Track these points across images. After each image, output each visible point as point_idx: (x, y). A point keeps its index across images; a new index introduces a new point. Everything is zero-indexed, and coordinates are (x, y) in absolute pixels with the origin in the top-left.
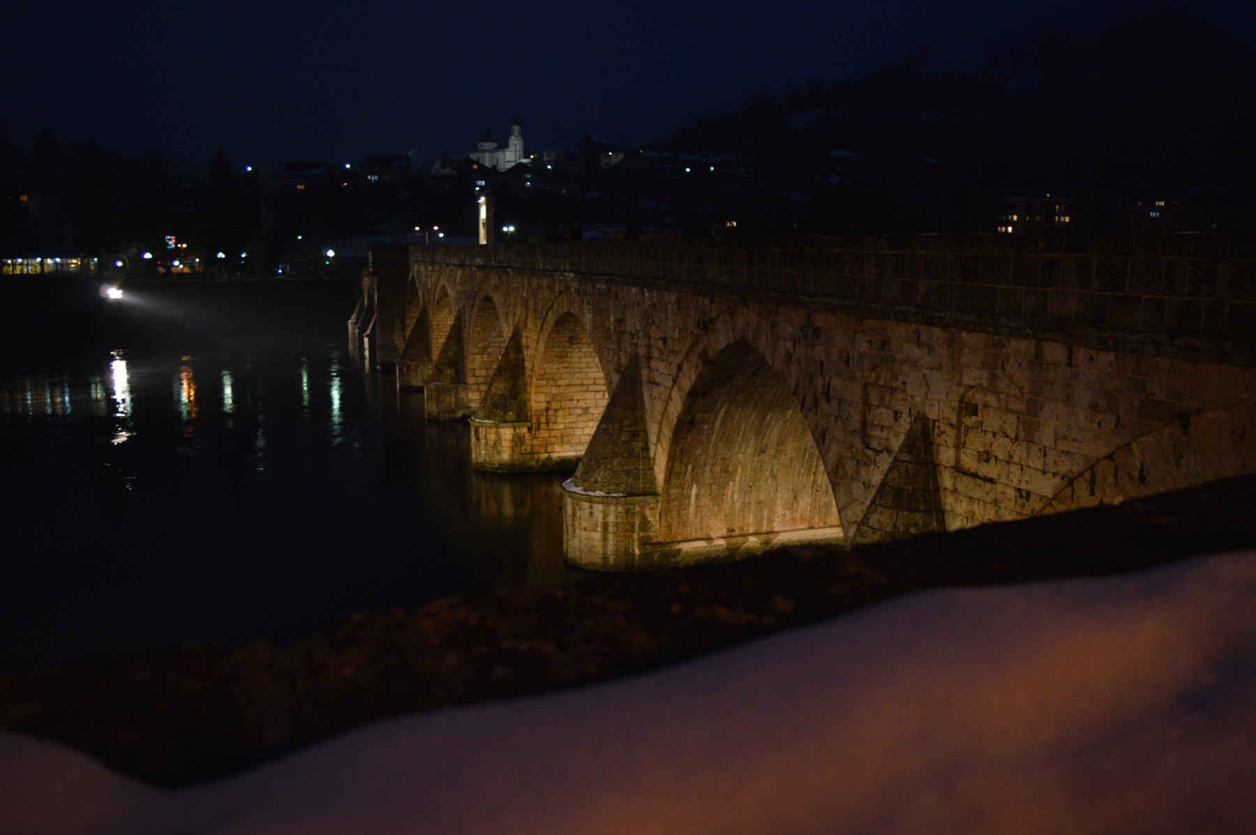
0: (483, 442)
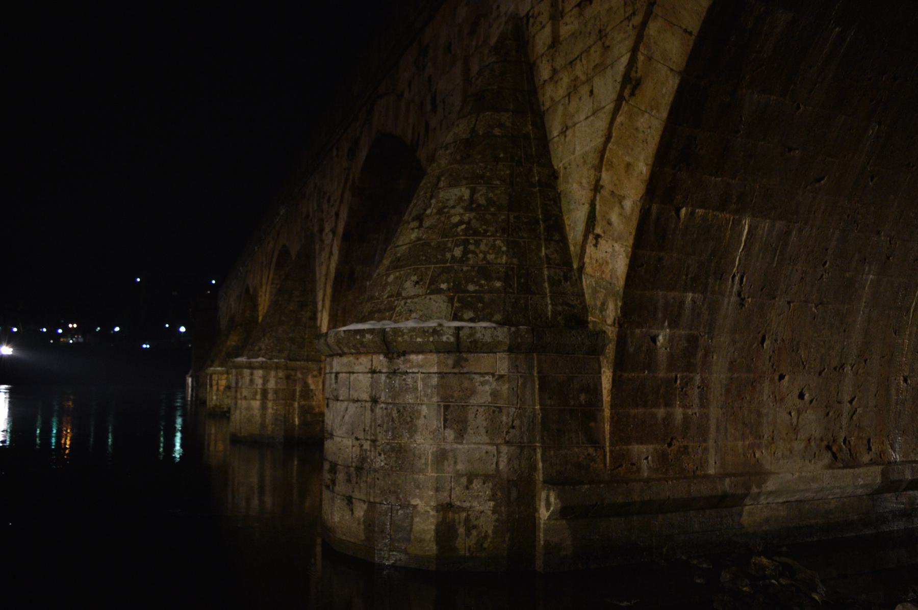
0: (215, 388)
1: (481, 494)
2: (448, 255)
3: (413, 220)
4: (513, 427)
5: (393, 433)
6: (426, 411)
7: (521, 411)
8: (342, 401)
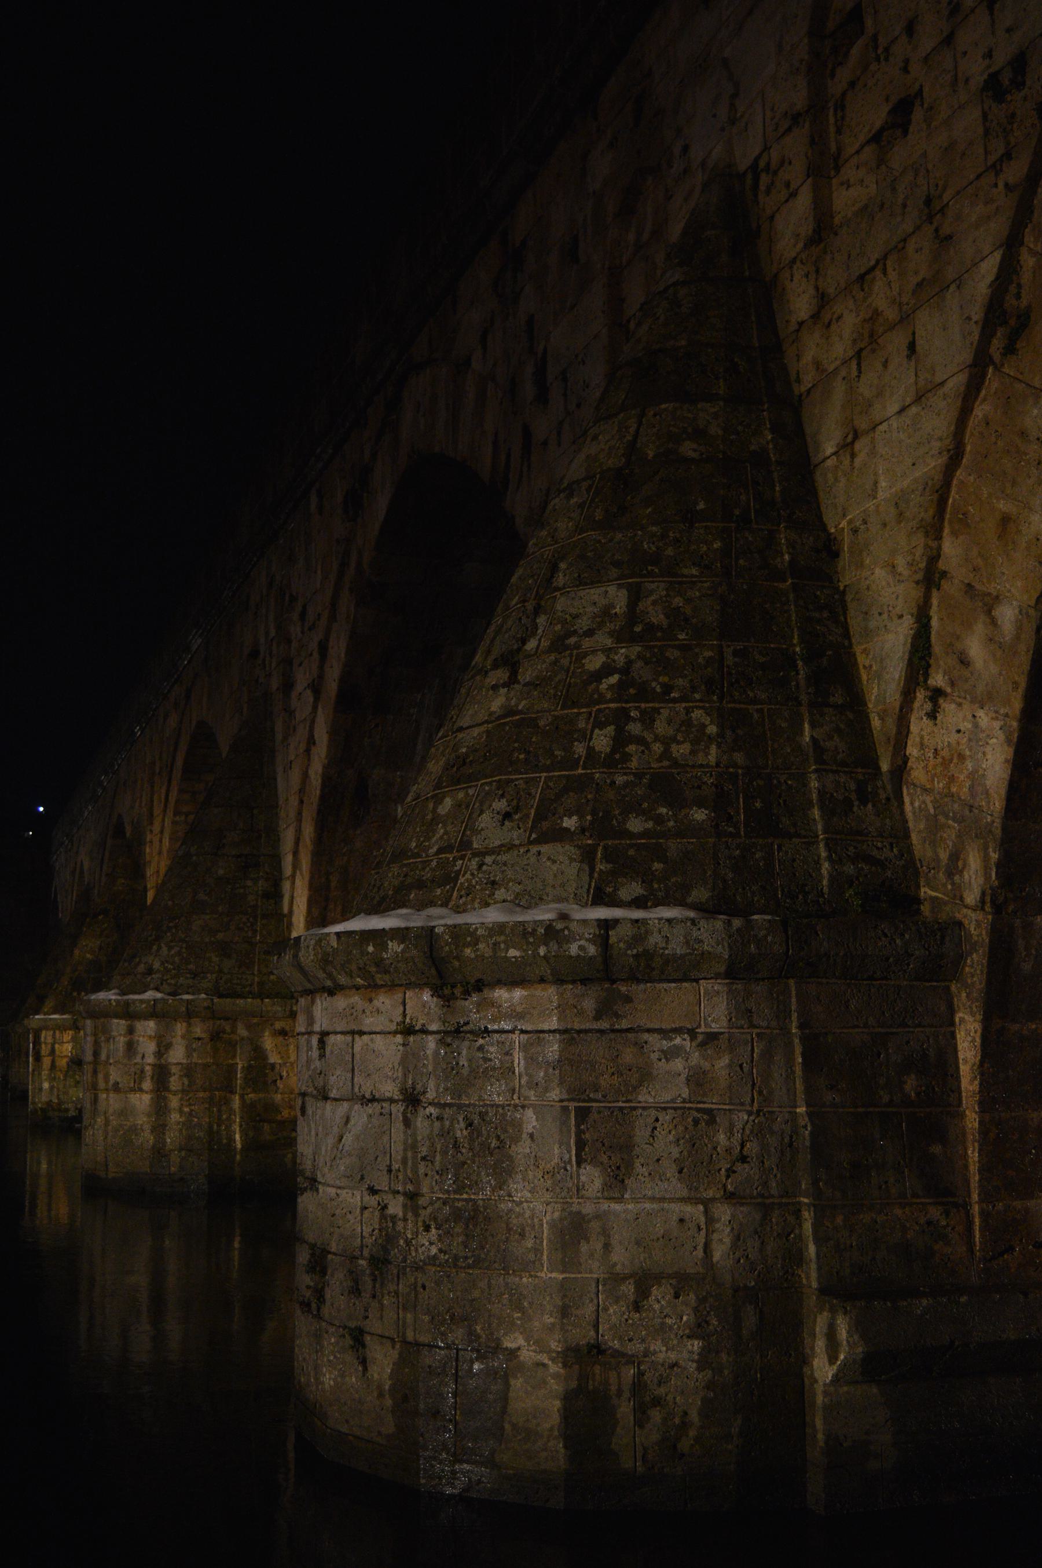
0: (47, 1062)
1: (669, 1321)
2: (580, 749)
3: (495, 666)
4: (743, 1159)
5: (456, 1175)
6: (535, 1124)
7: (762, 1119)
8: (336, 1100)
